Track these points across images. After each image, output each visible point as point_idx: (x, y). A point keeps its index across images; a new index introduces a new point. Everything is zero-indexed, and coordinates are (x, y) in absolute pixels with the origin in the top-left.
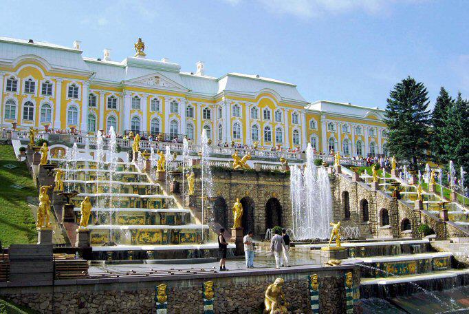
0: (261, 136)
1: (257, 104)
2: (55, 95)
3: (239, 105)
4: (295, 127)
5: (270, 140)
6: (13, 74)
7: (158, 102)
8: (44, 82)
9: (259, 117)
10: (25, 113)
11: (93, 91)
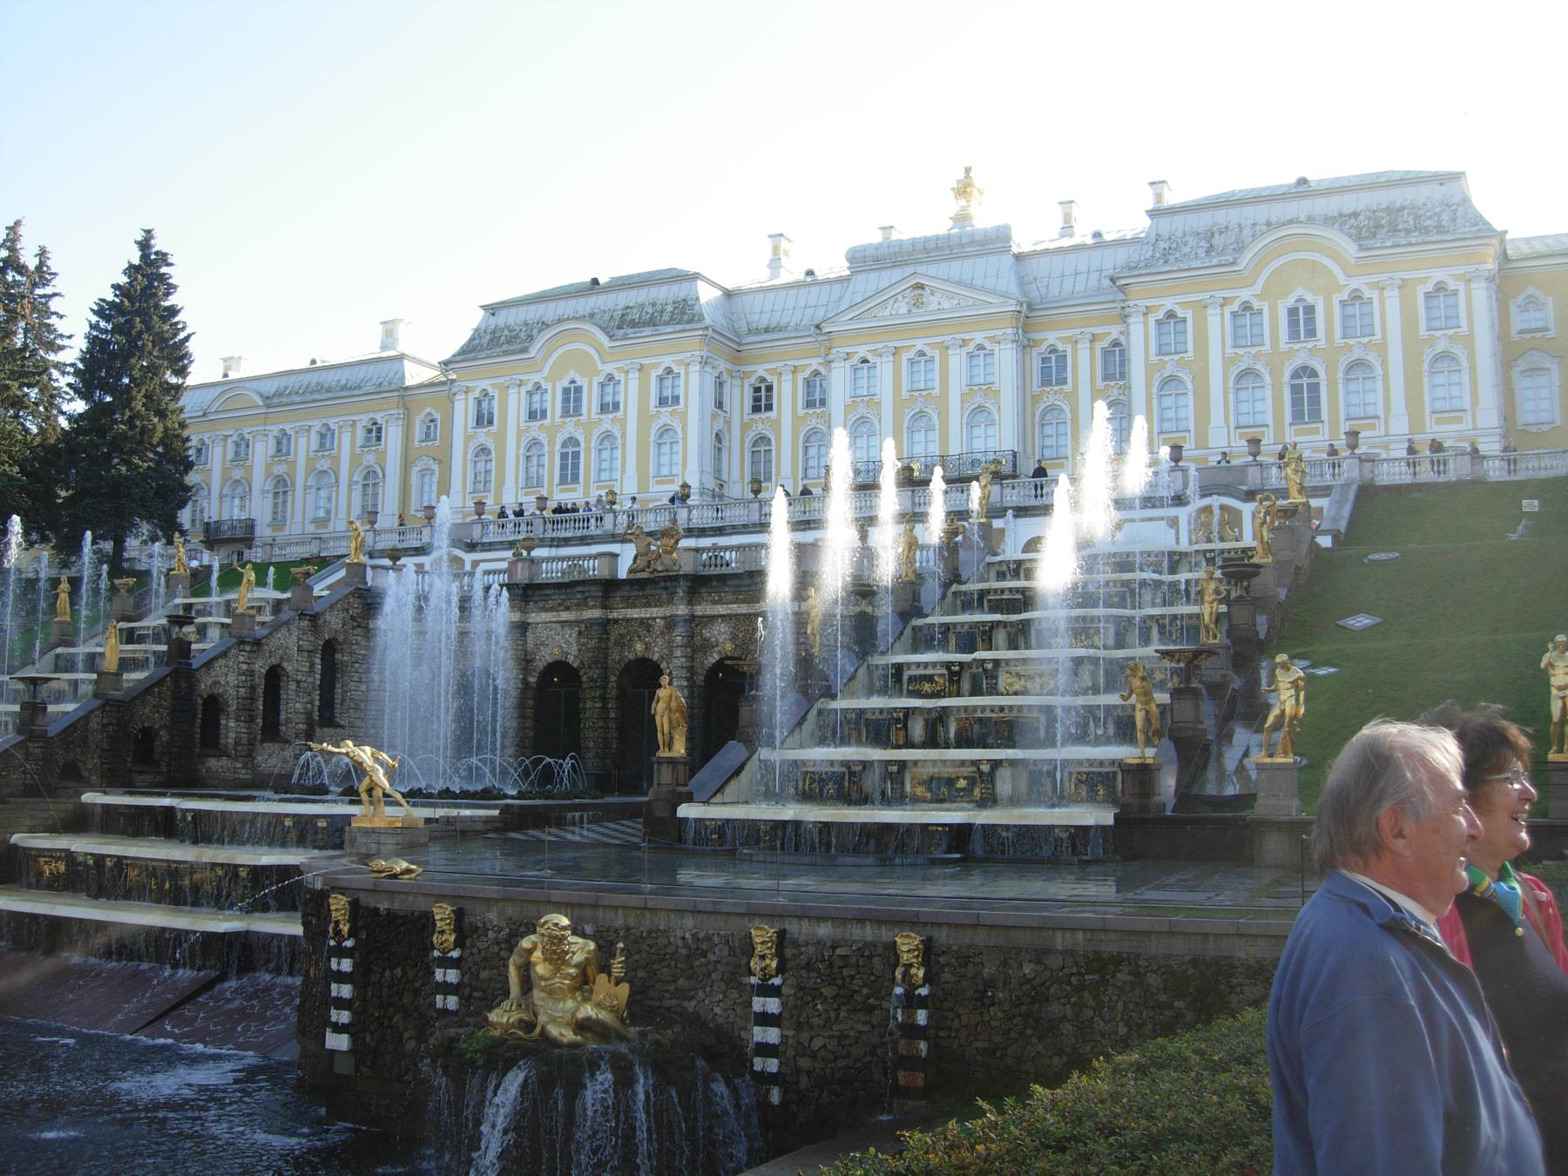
1: (1257, 289)
2: (625, 414)
3: (1180, 313)
4: (1442, 346)
5: (1315, 415)
6: (537, 378)
7: (932, 360)
9: (1267, 340)
10: (563, 467)
11: (761, 373)
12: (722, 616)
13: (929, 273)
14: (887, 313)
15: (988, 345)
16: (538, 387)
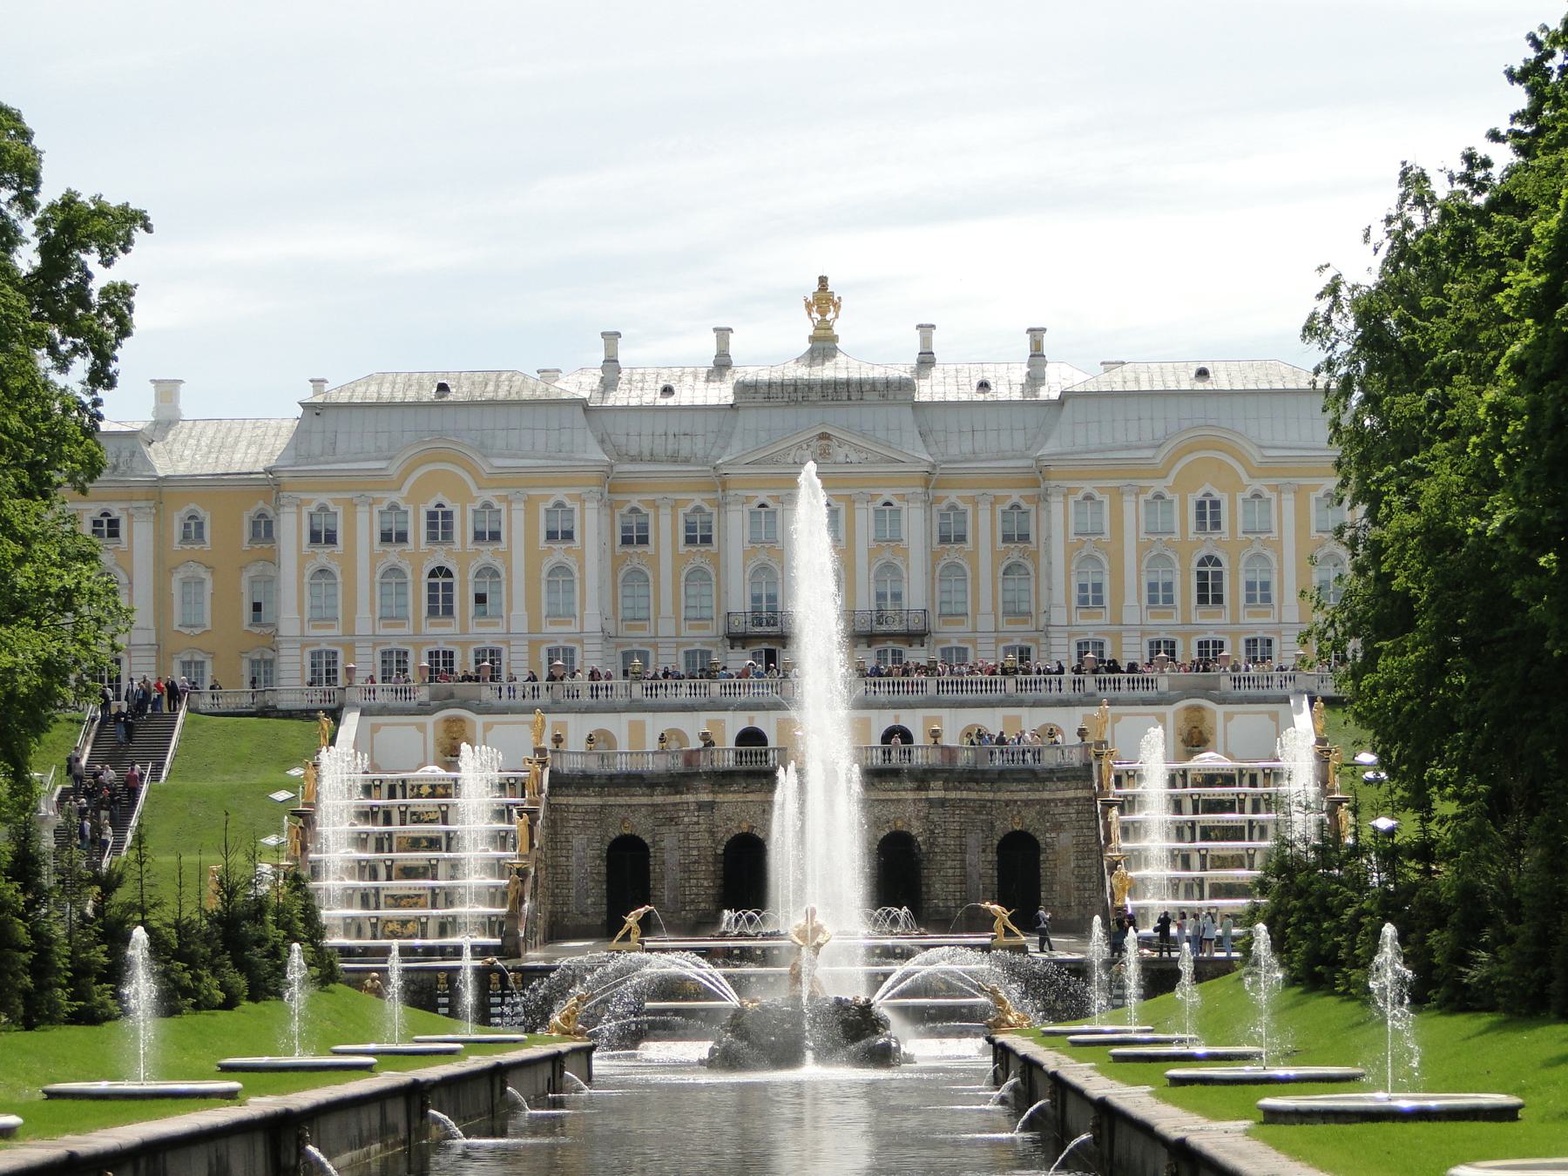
0: (1185, 588)
1: (1170, 481)
2: (510, 546)
3: (1098, 497)
5: (1218, 599)
6: (394, 497)
8: (477, 506)
9: (1177, 529)
10: (432, 599)
11: (635, 504)
12: (892, 800)
13: (834, 418)
14: (790, 460)
15: (896, 503)
16: (394, 507)
